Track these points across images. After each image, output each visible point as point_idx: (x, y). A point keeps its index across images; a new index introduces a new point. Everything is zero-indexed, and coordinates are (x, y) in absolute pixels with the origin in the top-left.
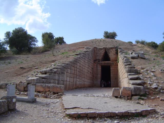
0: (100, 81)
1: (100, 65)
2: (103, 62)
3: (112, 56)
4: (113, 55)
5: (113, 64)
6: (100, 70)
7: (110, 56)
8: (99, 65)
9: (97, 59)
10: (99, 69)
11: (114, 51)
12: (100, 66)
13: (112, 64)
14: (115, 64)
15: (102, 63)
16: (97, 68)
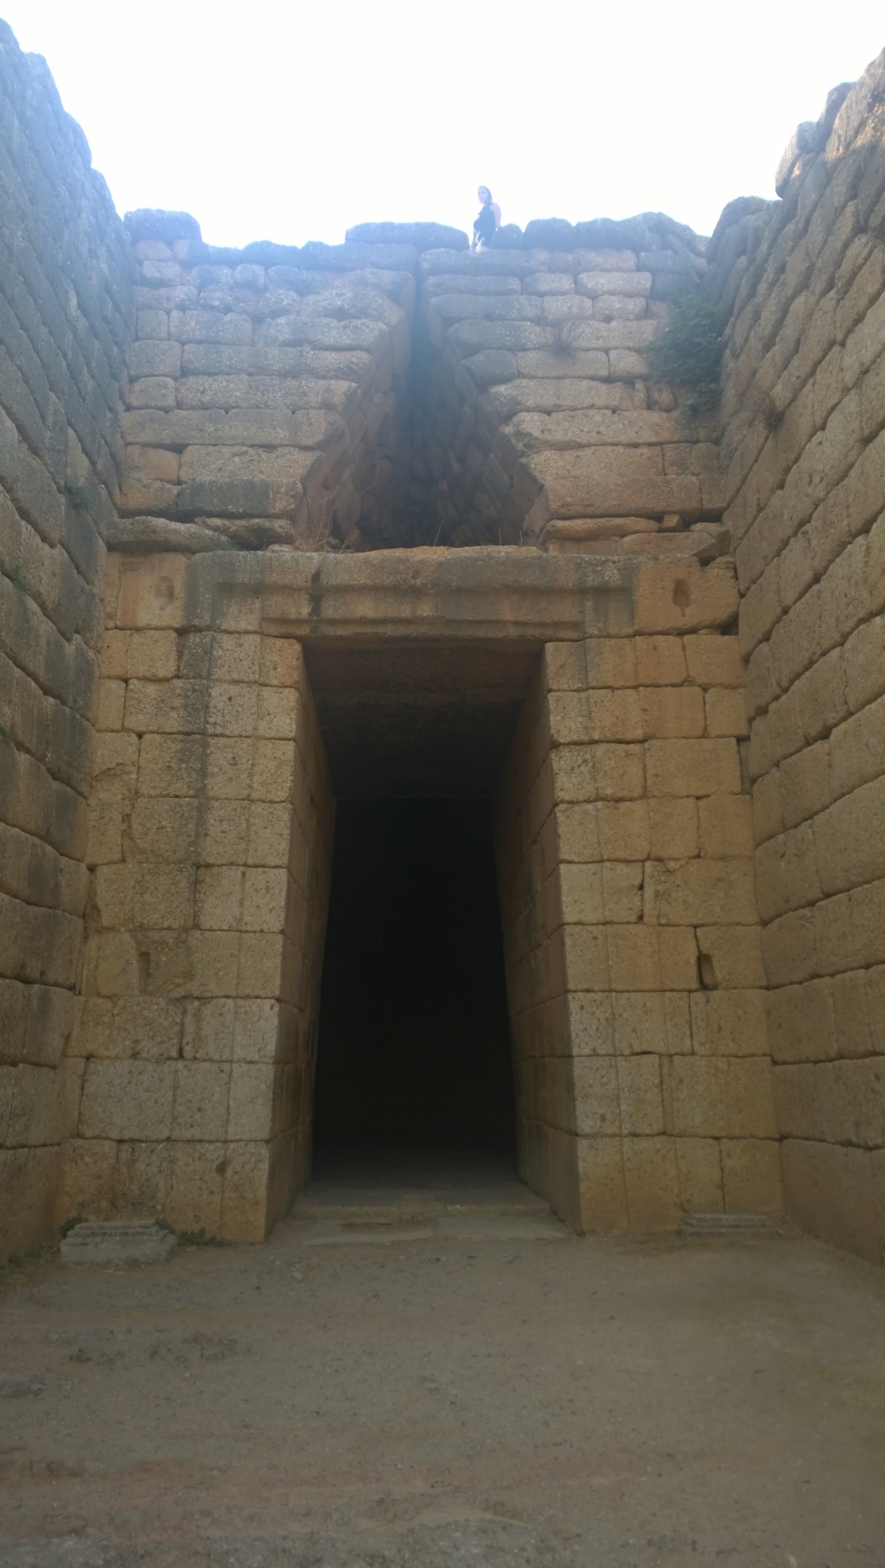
0: (271, 1048)
1: (279, 627)
2: (353, 565)
3: (560, 429)
4: (602, 394)
5: (620, 593)
6: (289, 750)
7: (530, 423)
8: (242, 616)
9: (205, 477)
10: (264, 725)
11: (616, 304)
12: (286, 659)
13: (581, 591)
14: (654, 605)
15: (317, 590)
16: (198, 705)
